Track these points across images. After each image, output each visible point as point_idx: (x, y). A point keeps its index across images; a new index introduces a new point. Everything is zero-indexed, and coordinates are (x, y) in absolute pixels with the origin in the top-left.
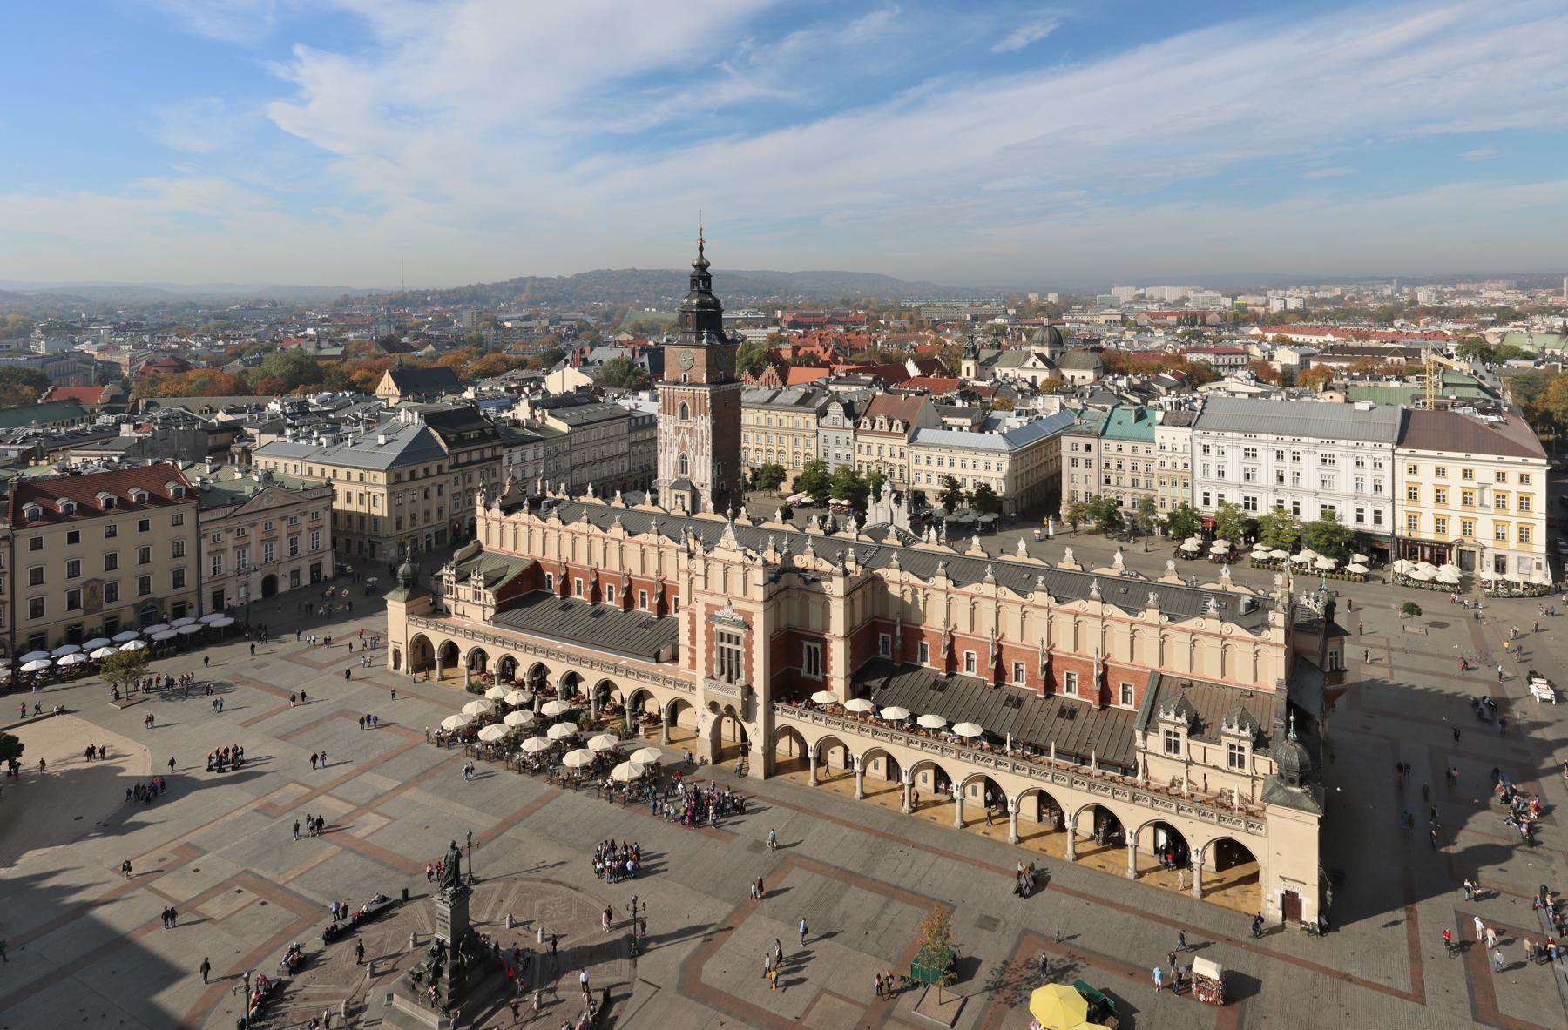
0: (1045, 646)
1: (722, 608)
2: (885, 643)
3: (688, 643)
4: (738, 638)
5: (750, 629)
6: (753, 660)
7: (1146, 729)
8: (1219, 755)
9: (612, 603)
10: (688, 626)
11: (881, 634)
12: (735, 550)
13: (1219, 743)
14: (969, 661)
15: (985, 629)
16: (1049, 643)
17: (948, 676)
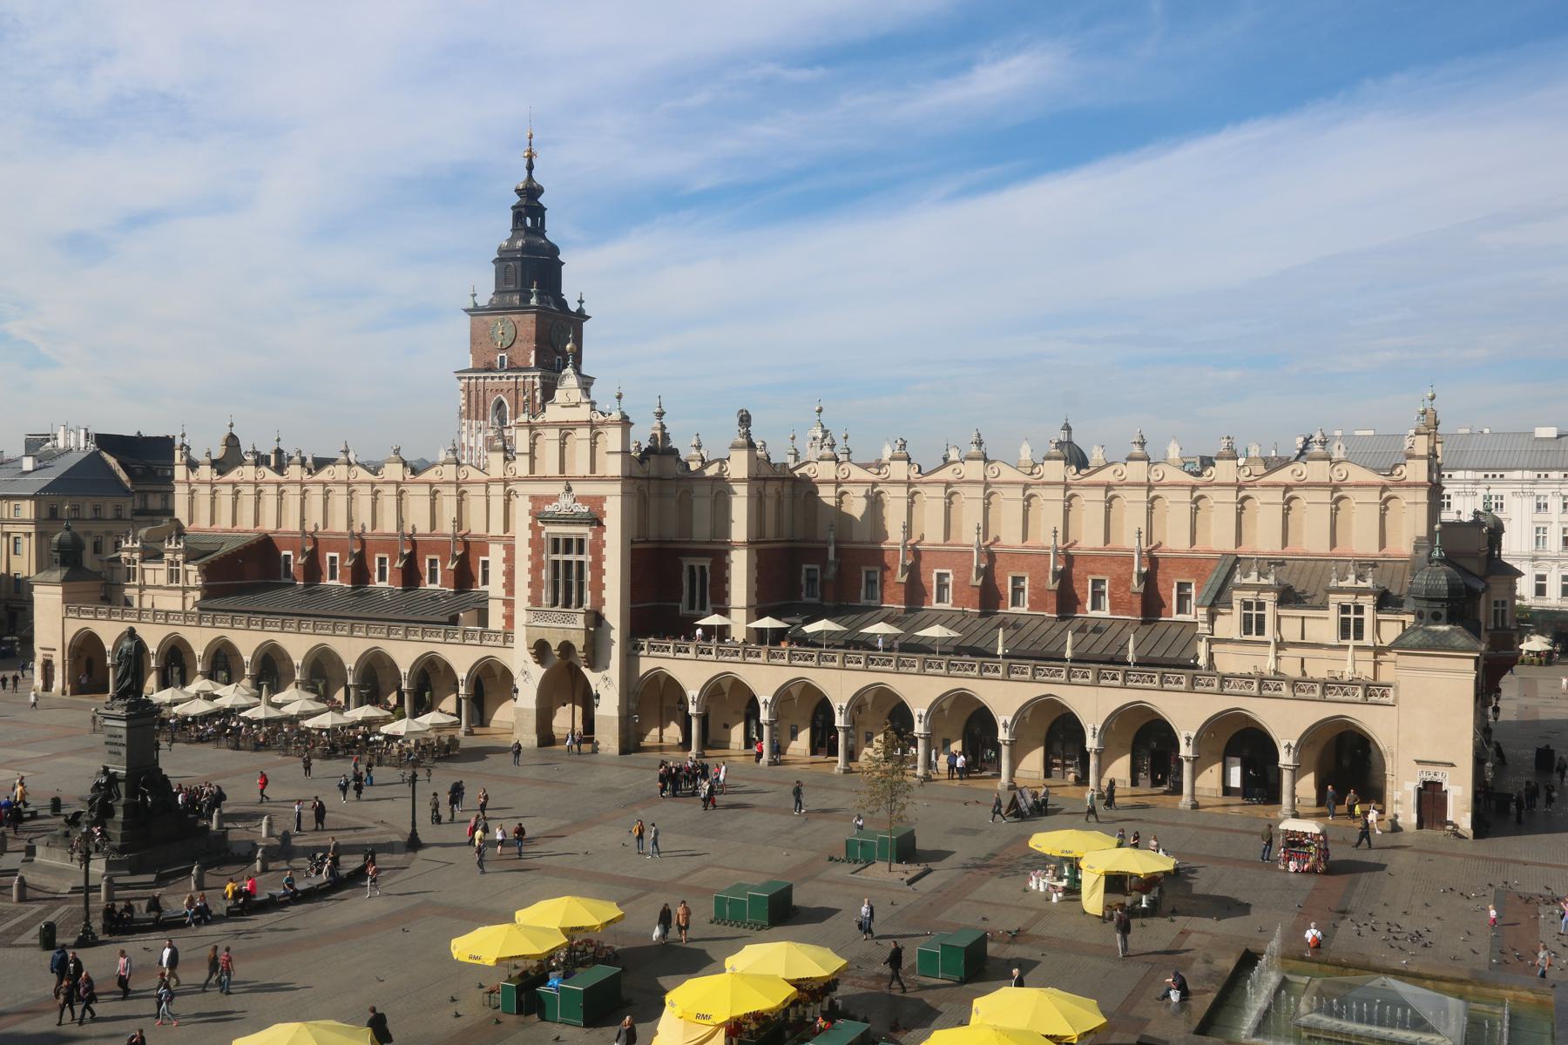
0: (1060, 543)
1: (555, 498)
2: (812, 581)
3: (502, 593)
4: (581, 542)
5: (600, 524)
6: (603, 572)
7: (1212, 605)
8: (1324, 626)
9: (383, 584)
10: (503, 567)
11: (805, 567)
12: (577, 405)
13: (1325, 607)
14: (942, 586)
15: (968, 535)
16: (1066, 539)
17: (907, 611)
